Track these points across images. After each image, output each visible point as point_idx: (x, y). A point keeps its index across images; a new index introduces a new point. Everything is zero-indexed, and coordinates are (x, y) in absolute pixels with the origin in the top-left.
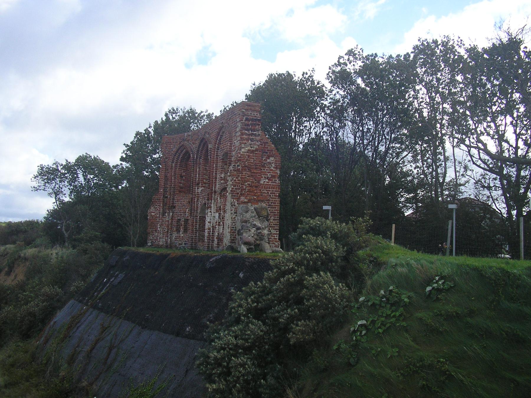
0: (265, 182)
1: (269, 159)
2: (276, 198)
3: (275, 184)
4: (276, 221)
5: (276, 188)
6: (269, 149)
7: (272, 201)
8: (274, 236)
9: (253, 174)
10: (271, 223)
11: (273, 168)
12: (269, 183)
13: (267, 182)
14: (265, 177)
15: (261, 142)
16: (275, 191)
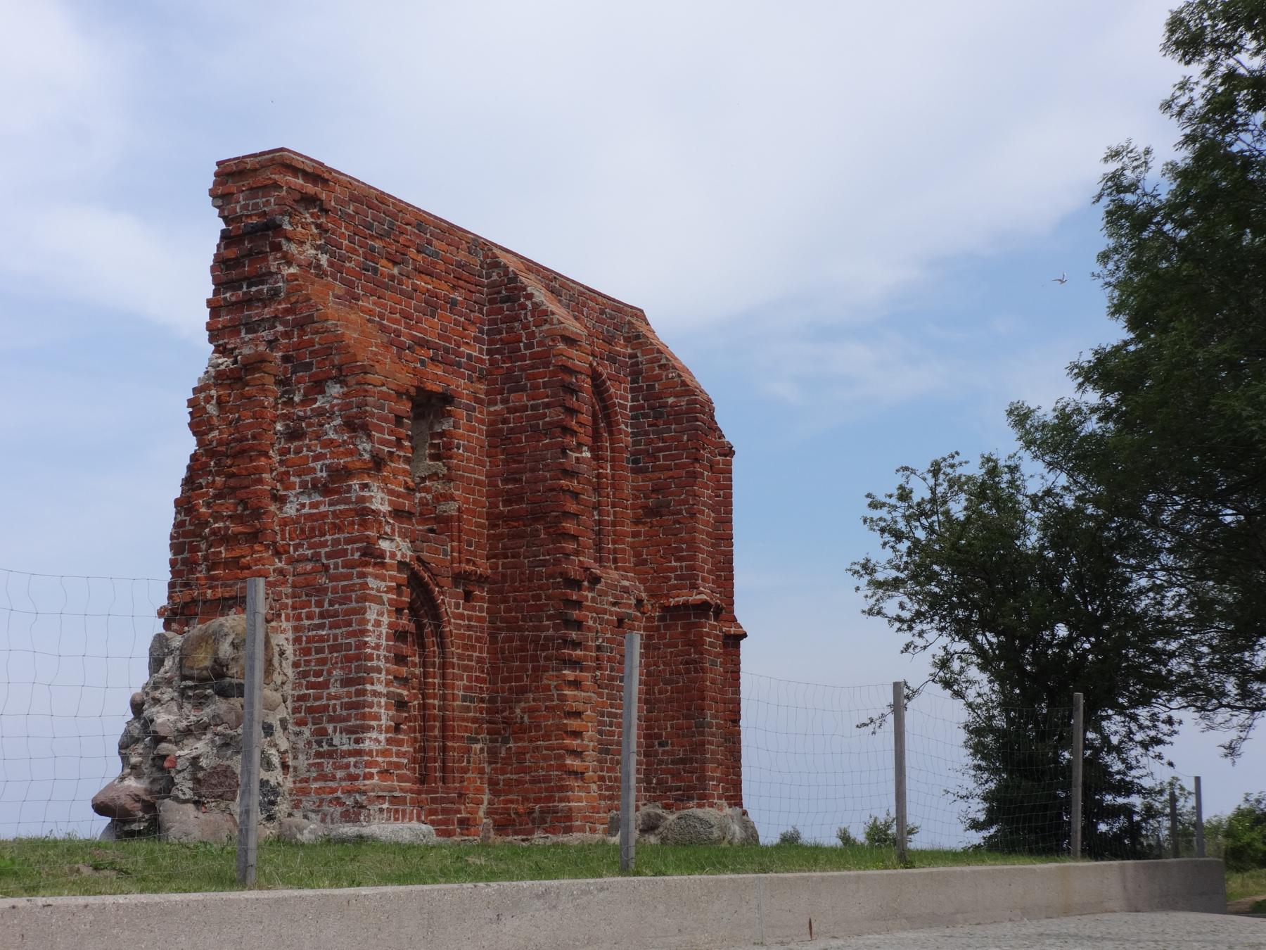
0: (303, 506)
1: (324, 392)
2: (348, 577)
3: (342, 507)
4: (353, 689)
5: (353, 523)
6: (317, 346)
7: (335, 590)
8: (348, 766)
9: (232, 482)
10: (334, 702)
11: (336, 431)
12: (323, 509)
13: (313, 505)
14: (304, 485)
15: (285, 324)
16: (348, 541)
